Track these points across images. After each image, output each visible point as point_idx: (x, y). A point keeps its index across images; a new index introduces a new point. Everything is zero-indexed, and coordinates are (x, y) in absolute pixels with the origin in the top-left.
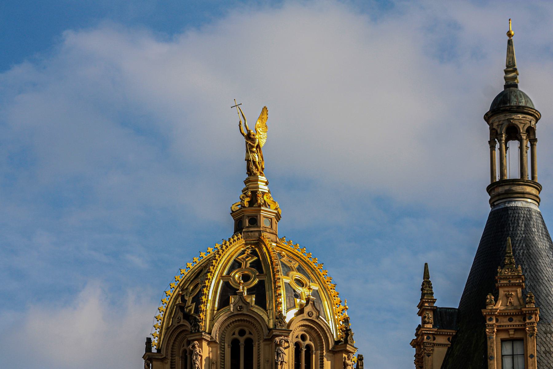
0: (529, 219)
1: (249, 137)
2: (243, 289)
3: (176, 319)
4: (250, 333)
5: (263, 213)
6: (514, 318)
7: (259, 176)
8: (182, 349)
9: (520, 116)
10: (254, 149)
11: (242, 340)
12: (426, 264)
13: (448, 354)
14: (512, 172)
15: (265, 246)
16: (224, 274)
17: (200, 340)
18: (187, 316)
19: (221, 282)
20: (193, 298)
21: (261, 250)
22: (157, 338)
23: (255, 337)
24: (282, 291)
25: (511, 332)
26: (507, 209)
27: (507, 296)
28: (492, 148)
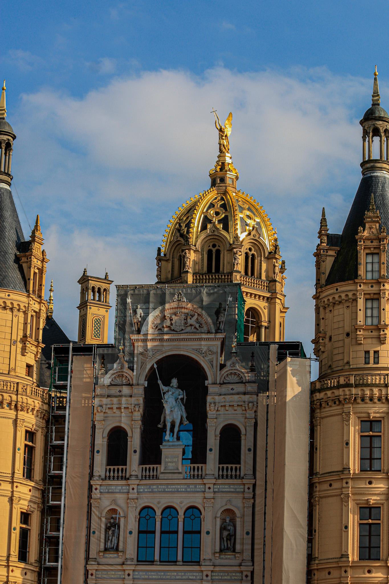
0: (384, 184)
1: (221, 130)
2: (215, 220)
3: (176, 237)
4: (219, 246)
5: (228, 176)
6: (374, 241)
7: (226, 154)
8: (179, 254)
9: (381, 122)
10: (224, 138)
11: (214, 250)
12: (324, 208)
13: (335, 262)
14: (375, 156)
15: (229, 195)
16: (205, 211)
17: (189, 249)
18: (182, 235)
19: (203, 216)
20: (186, 225)
21: (226, 197)
22: (164, 248)
23: (221, 249)
24: (239, 222)
25: (372, 249)
26: (372, 177)
27: (371, 228)
28: (364, 140)
